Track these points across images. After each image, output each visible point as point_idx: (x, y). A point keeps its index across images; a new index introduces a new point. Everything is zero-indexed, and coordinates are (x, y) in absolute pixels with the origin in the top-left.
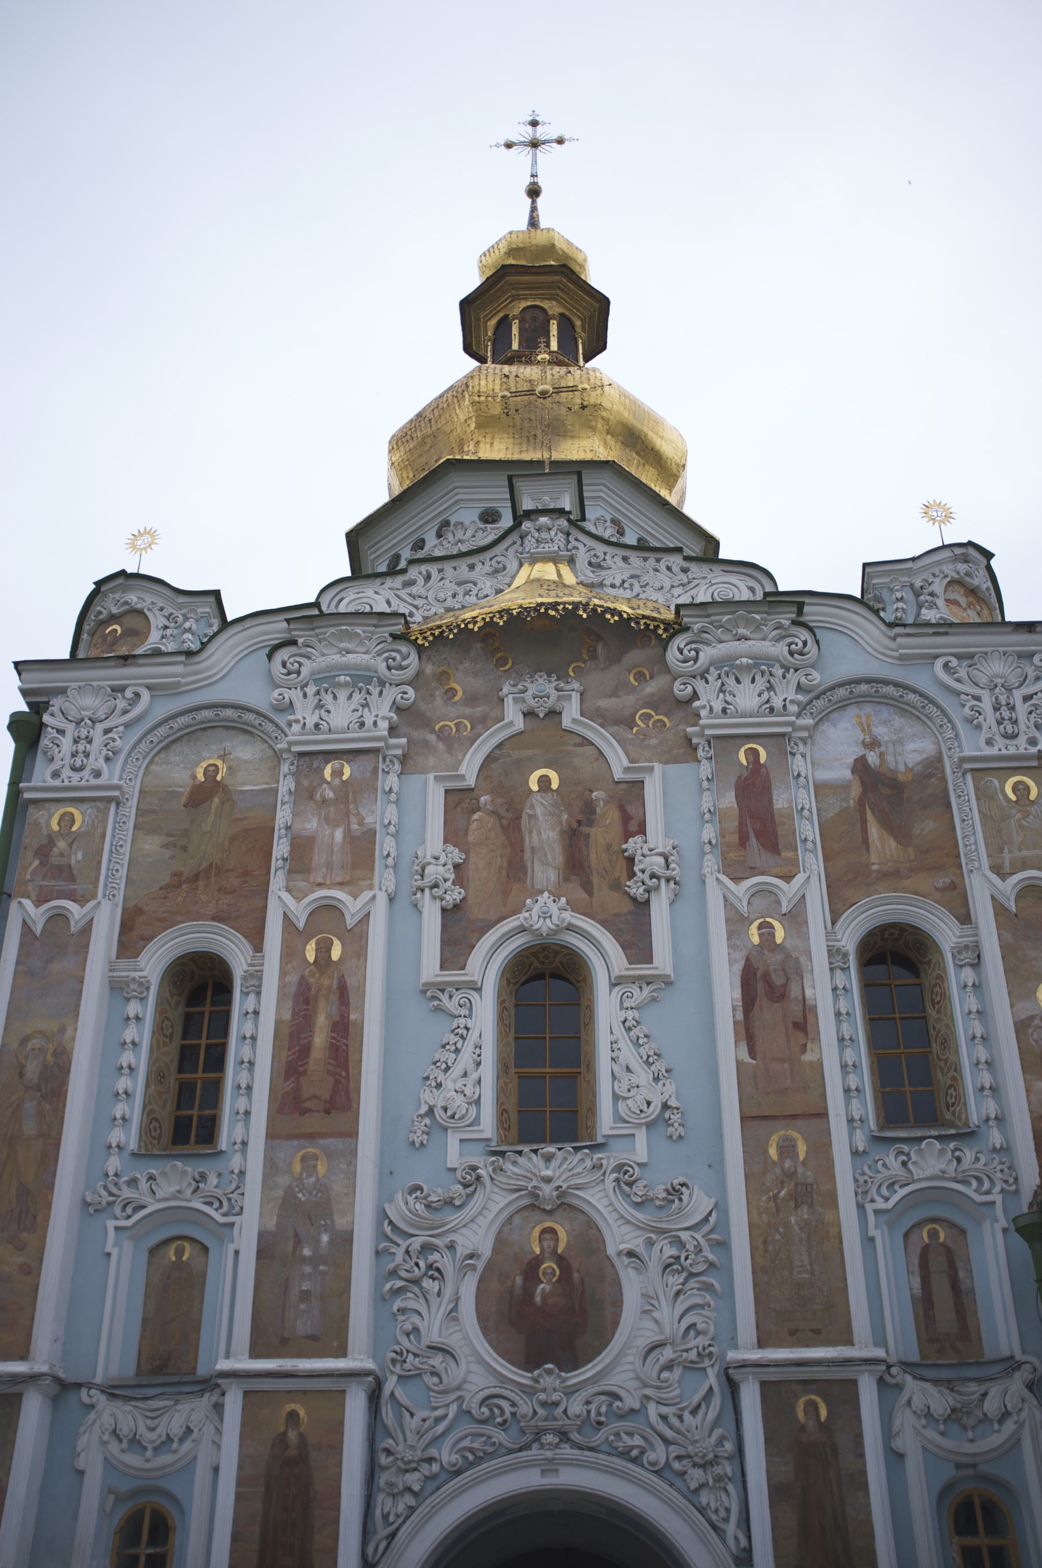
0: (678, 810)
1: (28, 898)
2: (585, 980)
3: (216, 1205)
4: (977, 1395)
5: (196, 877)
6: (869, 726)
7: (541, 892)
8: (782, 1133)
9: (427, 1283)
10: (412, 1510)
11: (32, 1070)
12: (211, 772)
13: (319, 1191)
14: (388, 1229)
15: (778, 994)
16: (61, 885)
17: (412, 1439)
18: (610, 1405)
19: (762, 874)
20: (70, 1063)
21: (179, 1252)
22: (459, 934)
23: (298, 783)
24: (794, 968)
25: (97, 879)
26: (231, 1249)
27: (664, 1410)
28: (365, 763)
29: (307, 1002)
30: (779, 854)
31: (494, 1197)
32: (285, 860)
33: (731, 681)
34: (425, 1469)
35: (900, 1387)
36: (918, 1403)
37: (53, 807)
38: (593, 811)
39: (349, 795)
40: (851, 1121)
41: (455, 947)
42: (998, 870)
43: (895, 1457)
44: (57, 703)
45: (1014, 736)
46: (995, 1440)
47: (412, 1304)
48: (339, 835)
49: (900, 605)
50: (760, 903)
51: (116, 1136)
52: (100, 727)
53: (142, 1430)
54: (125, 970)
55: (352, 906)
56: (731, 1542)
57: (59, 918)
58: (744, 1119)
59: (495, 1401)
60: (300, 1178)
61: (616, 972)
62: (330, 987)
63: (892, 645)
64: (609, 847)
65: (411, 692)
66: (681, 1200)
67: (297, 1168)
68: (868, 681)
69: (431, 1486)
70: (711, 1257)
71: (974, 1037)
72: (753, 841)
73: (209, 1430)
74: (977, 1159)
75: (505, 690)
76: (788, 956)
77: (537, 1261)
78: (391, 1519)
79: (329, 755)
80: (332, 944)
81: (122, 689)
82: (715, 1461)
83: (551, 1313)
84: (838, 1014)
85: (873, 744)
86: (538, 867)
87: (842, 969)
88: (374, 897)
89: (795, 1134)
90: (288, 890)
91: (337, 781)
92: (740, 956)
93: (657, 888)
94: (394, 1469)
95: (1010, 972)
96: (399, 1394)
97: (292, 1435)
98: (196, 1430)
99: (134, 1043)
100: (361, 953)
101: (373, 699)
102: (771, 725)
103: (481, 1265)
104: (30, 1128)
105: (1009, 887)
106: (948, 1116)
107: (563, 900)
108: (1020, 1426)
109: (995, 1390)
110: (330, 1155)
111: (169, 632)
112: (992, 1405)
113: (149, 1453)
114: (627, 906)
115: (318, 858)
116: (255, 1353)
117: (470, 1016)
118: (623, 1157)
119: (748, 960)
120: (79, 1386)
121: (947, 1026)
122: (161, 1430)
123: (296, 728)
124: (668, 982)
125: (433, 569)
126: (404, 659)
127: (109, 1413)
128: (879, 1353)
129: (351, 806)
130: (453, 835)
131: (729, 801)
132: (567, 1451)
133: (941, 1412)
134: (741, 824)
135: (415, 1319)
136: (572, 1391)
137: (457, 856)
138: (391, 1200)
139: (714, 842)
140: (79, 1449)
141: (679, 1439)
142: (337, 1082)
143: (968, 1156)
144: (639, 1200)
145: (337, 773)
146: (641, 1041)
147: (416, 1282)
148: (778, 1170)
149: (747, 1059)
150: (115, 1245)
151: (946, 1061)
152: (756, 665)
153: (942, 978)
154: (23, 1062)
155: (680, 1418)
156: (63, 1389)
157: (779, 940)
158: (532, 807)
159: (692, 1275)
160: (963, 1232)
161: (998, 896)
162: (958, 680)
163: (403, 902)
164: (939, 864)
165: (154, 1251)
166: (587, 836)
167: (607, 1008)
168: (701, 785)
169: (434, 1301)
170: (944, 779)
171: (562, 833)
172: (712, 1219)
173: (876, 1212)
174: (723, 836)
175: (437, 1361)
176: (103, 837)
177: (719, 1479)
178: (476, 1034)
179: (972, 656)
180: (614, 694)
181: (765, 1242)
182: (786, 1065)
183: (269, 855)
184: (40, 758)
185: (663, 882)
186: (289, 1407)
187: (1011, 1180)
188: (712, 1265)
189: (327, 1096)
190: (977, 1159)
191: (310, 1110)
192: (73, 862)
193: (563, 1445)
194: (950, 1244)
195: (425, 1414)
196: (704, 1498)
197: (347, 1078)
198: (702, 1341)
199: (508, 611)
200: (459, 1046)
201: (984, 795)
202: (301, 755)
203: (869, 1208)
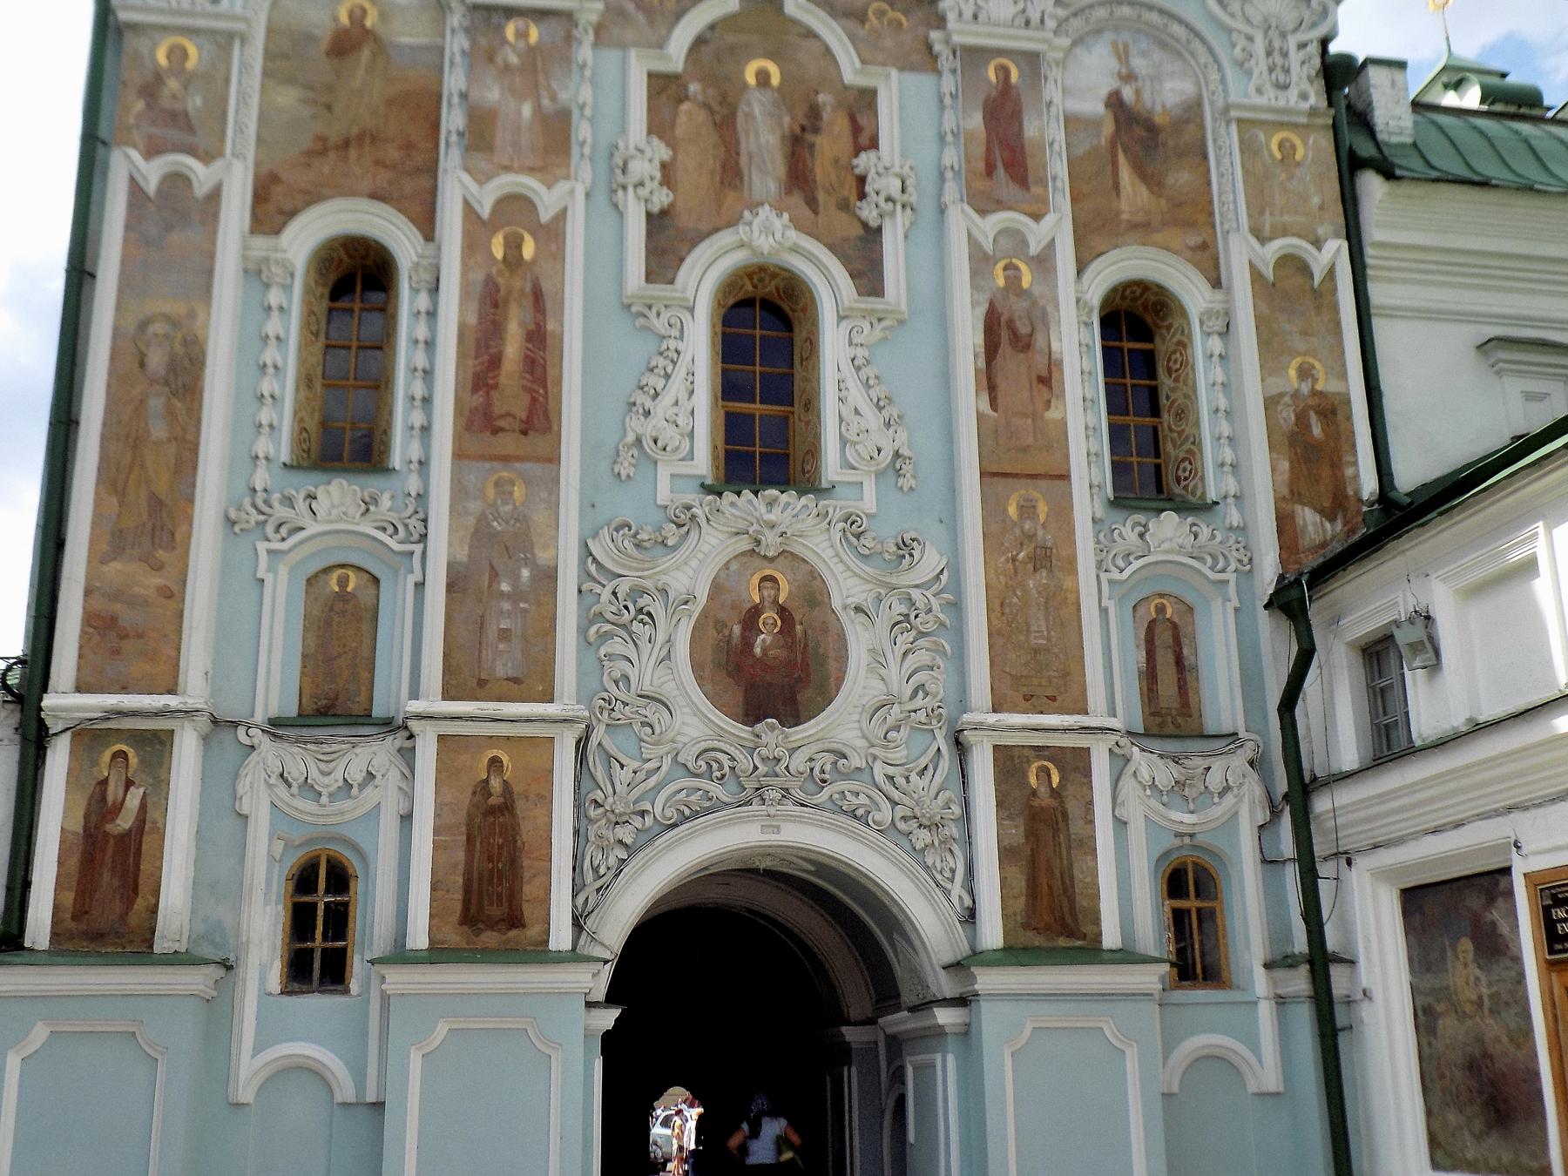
1: (135, 146)
2: (804, 309)
3: (390, 530)
4: (1201, 770)
5: (346, 144)
6: (1127, 53)
8: (1023, 492)
9: (636, 626)
11: (157, 360)
12: (358, 15)
13: (517, 520)
14: (592, 568)
15: (1023, 344)
16: (175, 135)
18: (835, 763)
19: (1010, 208)
20: (203, 354)
21: (343, 582)
22: (667, 243)
23: (473, 41)
24: (1041, 317)
25: (223, 133)
26: (411, 580)
27: (891, 771)
28: (556, 27)
29: (496, 305)
30: (1028, 189)
31: (708, 538)
32: (461, 134)
34: (637, 822)
36: (1145, 775)
39: (537, 68)
43: (1121, 824)
45: (1286, 87)
48: (527, 110)
50: (1004, 243)
51: (263, 446)
53: (314, 773)
55: (548, 199)
56: (955, 900)
57: (177, 181)
59: (713, 754)
60: (494, 505)
62: (522, 291)
64: (836, 161)
66: (911, 555)
67: (491, 492)
70: (942, 616)
71: (1217, 410)
72: (1001, 172)
73: (391, 779)
74: (1213, 537)
76: (1034, 303)
77: (755, 612)
78: (602, 871)
79: (510, 12)
80: (522, 238)
83: (772, 670)
85: (1129, 77)
87: (1086, 324)
88: (572, 192)
89: (1037, 495)
90: (468, 170)
91: (522, 44)
93: (893, 214)
94: (603, 822)
95: (1264, 344)
96: (607, 743)
97: (496, 784)
98: (379, 776)
99: (278, 338)
100: (559, 256)
102: (1024, 42)
103: (697, 609)
104: (159, 430)
106: (1177, 490)
107: (786, 216)
108: (1240, 798)
109: (1217, 765)
110: (528, 483)
112: (1215, 780)
113: (324, 799)
114: (860, 231)
115: (502, 137)
116: (447, 695)
117: (682, 338)
118: (850, 506)
119: (991, 303)
120: (235, 725)
121: (1186, 396)
129: (541, 77)
130: (659, 126)
131: (976, 121)
132: (790, 807)
133: (1166, 782)
134: (989, 150)
138: (595, 535)
139: (956, 167)
140: (240, 792)
141: (906, 800)
142: (534, 400)
143: (1205, 532)
144: (867, 552)
145: (523, 34)
146: (871, 382)
148: (1017, 531)
149: (991, 412)
150: (269, 570)
151: (1181, 433)
153: (1183, 345)
154: (143, 348)
155: (907, 778)
157: (1025, 285)
158: (749, 104)
159: (922, 635)
160: (1191, 609)
161: (1257, 262)
162: (1232, 15)
163: (601, 198)
166: (812, 146)
167: (835, 347)
168: (941, 101)
169: (645, 647)
170: (1202, 126)
171: (783, 137)
172: (944, 578)
173: (1110, 582)
174: (968, 161)
176: (227, 81)
178: (689, 358)
181: (1002, 604)
182: (1029, 421)
183: (436, 126)
185: (899, 207)
186: (495, 752)
187: (1246, 560)
188: (942, 624)
189: (523, 415)
190: (1213, 537)
191: (502, 429)
192: (190, 108)
193: (785, 801)
194: (1176, 620)
195: (636, 765)
197: (546, 396)
198: (930, 702)
200: (669, 370)
201: (1248, 148)
203: (1104, 576)
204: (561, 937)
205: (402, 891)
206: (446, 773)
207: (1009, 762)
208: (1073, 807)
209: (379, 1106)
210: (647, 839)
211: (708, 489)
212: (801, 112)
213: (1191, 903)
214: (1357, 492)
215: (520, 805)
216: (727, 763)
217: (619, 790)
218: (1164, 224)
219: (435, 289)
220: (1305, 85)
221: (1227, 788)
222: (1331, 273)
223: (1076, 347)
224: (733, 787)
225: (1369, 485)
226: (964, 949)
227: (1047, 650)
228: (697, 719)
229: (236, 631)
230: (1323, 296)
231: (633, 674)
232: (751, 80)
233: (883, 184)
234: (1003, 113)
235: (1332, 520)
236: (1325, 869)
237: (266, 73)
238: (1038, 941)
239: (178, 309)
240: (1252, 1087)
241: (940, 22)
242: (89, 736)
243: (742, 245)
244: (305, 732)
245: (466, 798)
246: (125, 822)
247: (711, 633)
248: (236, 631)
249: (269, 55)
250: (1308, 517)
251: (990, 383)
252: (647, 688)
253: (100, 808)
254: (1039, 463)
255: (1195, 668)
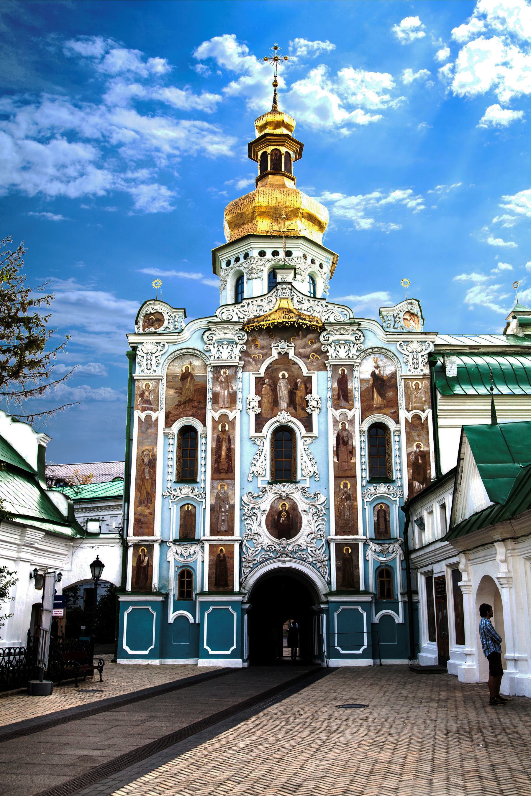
0: (322, 385)
5: (185, 402)
7: (282, 410)
9: (253, 517)
10: (250, 572)
11: (146, 460)
12: (187, 369)
15: (346, 443)
16: (148, 406)
17: (250, 555)
21: (188, 508)
24: (350, 436)
28: (233, 370)
33: (338, 347)
34: (254, 562)
35: (369, 545)
36: (373, 549)
37: (143, 381)
38: (297, 386)
39: (229, 380)
40: (362, 478)
41: (259, 427)
42: (408, 410)
43: (366, 561)
44: (140, 346)
45: (417, 368)
46: (391, 557)
47: (249, 522)
48: (226, 392)
49: (389, 322)
50: (342, 417)
51: (170, 477)
52: (154, 356)
54: (168, 430)
55: (231, 416)
57: (148, 417)
58: (335, 477)
61: (303, 435)
63: (385, 337)
64: (301, 397)
65: (245, 347)
67: (219, 488)
68: (377, 348)
69: (255, 566)
72: (342, 398)
73: (200, 553)
75: (273, 345)
77: (281, 512)
79: (222, 367)
81: (160, 343)
82: (323, 561)
84: (361, 448)
85: (377, 367)
86: (281, 402)
92: (336, 432)
96: (247, 544)
97: (222, 554)
101: (234, 349)
102: (349, 362)
103: (267, 513)
104: (147, 477)
105: (409, 416)
109: (392, 546)
111: (170, 321)
112: (390, 550)
115: (221, 399)
116: (211, 535)
119: (338, 433)
122: (188, 553)
123: (212, 358)
124: (316, 438)
125: (250, 301)
126: (243, 336)
127: (174, 548)
128: (365, 537)
131: (336, 385)
132: (288, 558)
134: (339, 393)
135: (250, 526)
136: (290, 544)
137: (259, 398)
145: (225, 373)
147: (250, 517)
152: (346, 343)
153: (390, 438)
156: (162, 543)
159: (320, 516)
160: (389, 507)
163: (244, 412)
164: (391, 406)
165: (181, 507)
167: (300, 445)
169: (255, 522)
170: (396, 379)
175: (256, 536)
177: (324, 565)
179: (408, 342)
180: (304, 348)
184: (137, 365)
189: (226, 468)
195: (252, 549)
196: (320, 570)
199: (274, 323)
201: (406, 386)
202: (214, 366)
203: (365, 500)
204: (236, 589)
205: (203, 579)
206: (211, 552)
207: (339, 547)
208: (354, 558)
209: (199, 624)
210: (256, 565)
211: (269, 483)
212: (293, 384)
213: (385, 579)
214: (430, 476)
215: (227, 559)
216: (274, 548)
217: (249, 554)
218: (385, 407)
219: (206, 438)
220: (423, 368)
221: (393, 552)
222: (427, 419)
223: (360, 443)
224: (275, 553)
225: (433, 474)
226: (328, 591)
227: (349, 520)
228: (266, 538)
229: (166, 521)
230: (424, 426)
231: (252, 528)
232: (280, 377)
233: (313, 403)
234: (343, 381)
235: (423, 485)
236: (411, 571)
237: (167, 386)
238: (344, 589)
239: (150, 448)
240: (397, 622)
241: (327, 358)
242: (136, 546)
243: (277, 421)
244: (181, 543)
245: (215, 558)
246: (145, 564)
247: (270, 518)
248: (166, 521)
249: (167, 382)
250: (417, 484)
251: (337, 453)
252: (256, 531)
253: (139, 561)
254: (348, 473)
255: (389, 521)
